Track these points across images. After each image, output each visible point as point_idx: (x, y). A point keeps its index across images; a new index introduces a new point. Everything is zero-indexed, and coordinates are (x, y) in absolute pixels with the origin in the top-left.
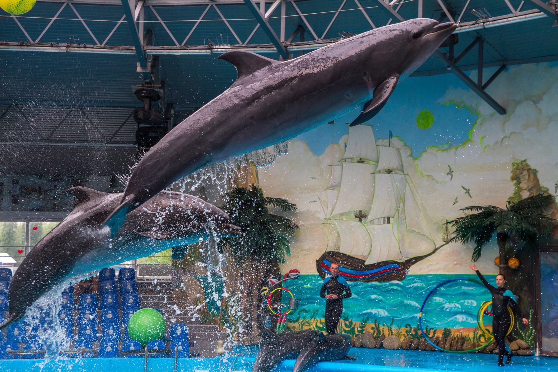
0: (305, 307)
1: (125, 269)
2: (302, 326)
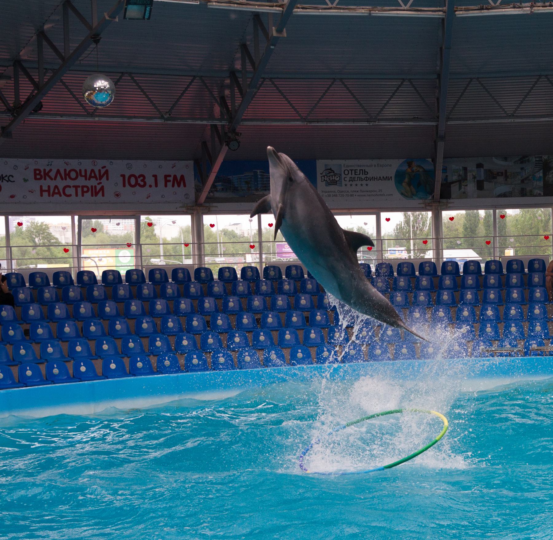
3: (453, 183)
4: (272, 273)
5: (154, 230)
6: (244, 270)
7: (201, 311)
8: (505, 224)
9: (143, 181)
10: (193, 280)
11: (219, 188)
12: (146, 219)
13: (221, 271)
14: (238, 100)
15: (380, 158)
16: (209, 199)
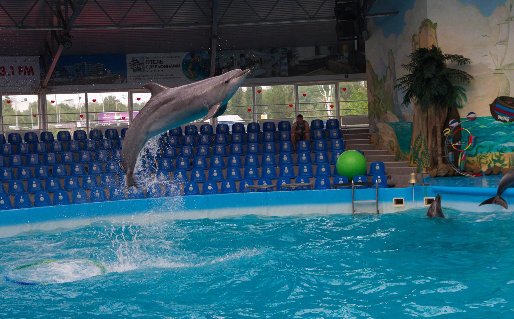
0: (481, 144)
1: (331, 120)
2: (480, 159)
3: (223, 68)
4: (96, 135)
5: (11, 105)
6: (76, 133)
7: (45, 162)
8: (261, 96)
9: (3, 71)
10: (39, 141)
11: (58, 75)
12: (6, 97)
13: (59, 134)
14: (70, 13)
15: (171, 52)
16: (51, 83)
